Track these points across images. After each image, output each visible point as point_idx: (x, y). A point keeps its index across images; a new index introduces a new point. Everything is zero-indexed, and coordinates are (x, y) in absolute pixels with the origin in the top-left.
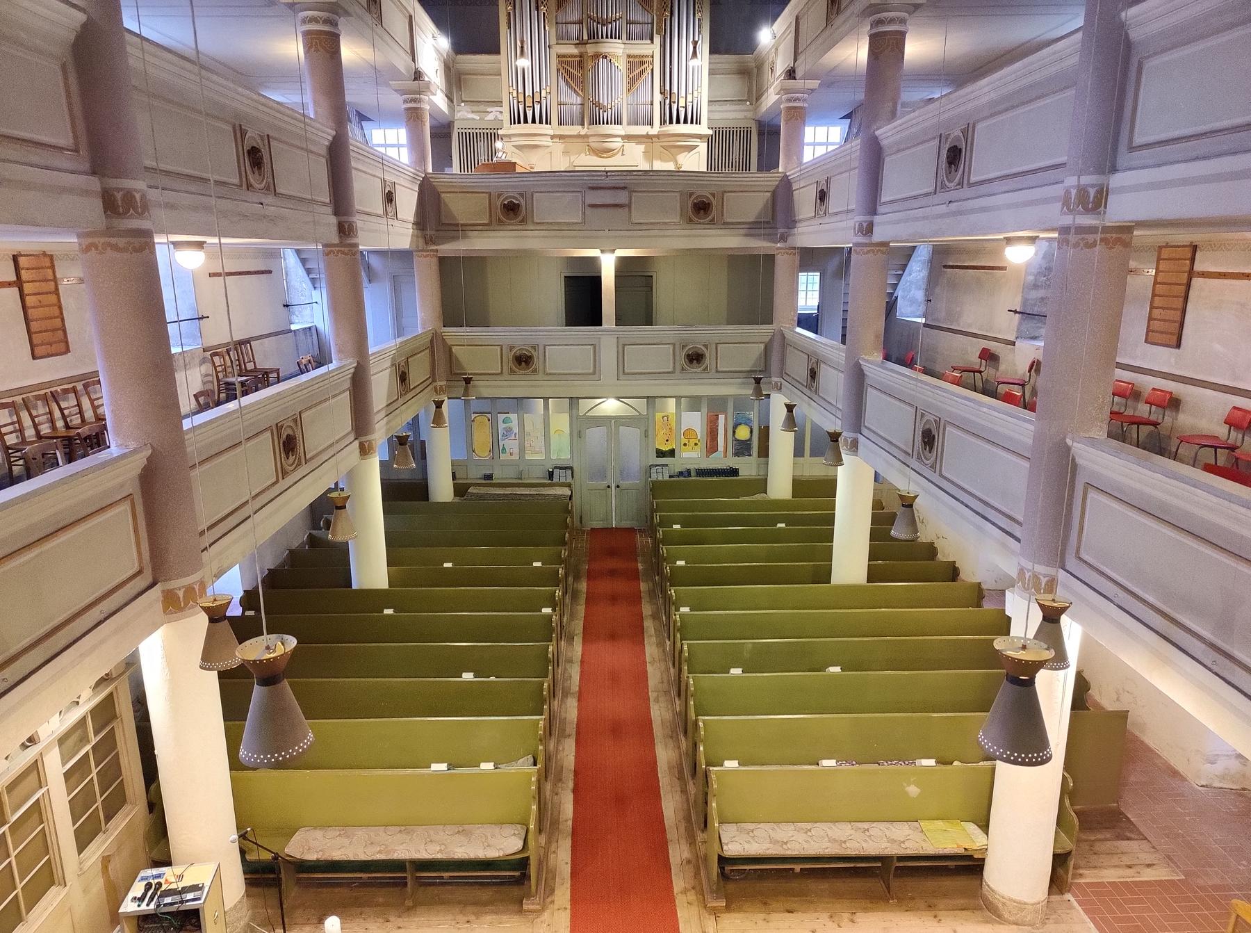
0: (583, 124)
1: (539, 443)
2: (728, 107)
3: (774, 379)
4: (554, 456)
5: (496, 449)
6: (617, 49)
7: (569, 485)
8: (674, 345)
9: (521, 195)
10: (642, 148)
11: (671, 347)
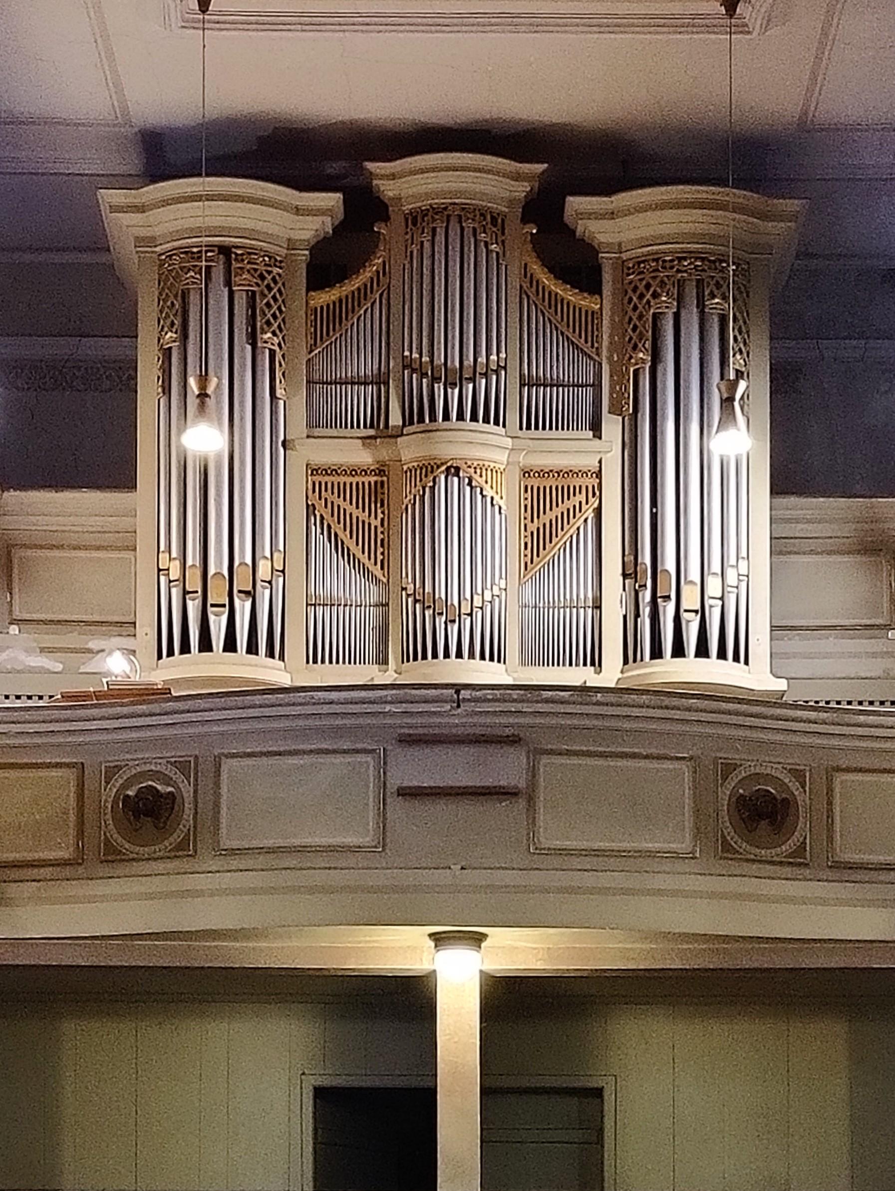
0: (383, 661)
6: (493, 450)
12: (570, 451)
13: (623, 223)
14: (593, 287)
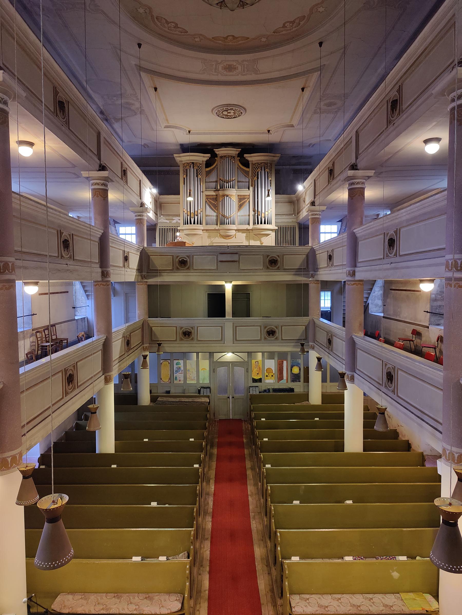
0: (217, 225)
1: (194, 375)
2: (284, 217)
3: (311, 343)
4: (201, 382)
5: (172, 378)
7: (208, 397)
8: (261, 326)
9: (188, 256)
10: (245, 235)
11: (259, 327)
12: (245, 192)
13: (253, 158)
14: (248, 167)
